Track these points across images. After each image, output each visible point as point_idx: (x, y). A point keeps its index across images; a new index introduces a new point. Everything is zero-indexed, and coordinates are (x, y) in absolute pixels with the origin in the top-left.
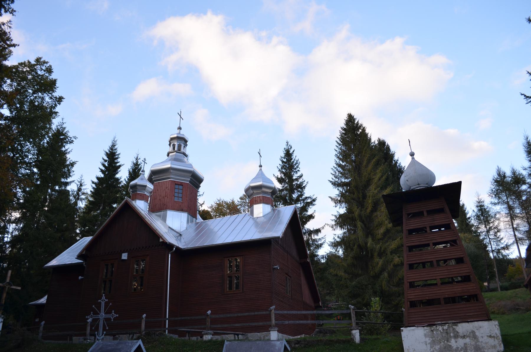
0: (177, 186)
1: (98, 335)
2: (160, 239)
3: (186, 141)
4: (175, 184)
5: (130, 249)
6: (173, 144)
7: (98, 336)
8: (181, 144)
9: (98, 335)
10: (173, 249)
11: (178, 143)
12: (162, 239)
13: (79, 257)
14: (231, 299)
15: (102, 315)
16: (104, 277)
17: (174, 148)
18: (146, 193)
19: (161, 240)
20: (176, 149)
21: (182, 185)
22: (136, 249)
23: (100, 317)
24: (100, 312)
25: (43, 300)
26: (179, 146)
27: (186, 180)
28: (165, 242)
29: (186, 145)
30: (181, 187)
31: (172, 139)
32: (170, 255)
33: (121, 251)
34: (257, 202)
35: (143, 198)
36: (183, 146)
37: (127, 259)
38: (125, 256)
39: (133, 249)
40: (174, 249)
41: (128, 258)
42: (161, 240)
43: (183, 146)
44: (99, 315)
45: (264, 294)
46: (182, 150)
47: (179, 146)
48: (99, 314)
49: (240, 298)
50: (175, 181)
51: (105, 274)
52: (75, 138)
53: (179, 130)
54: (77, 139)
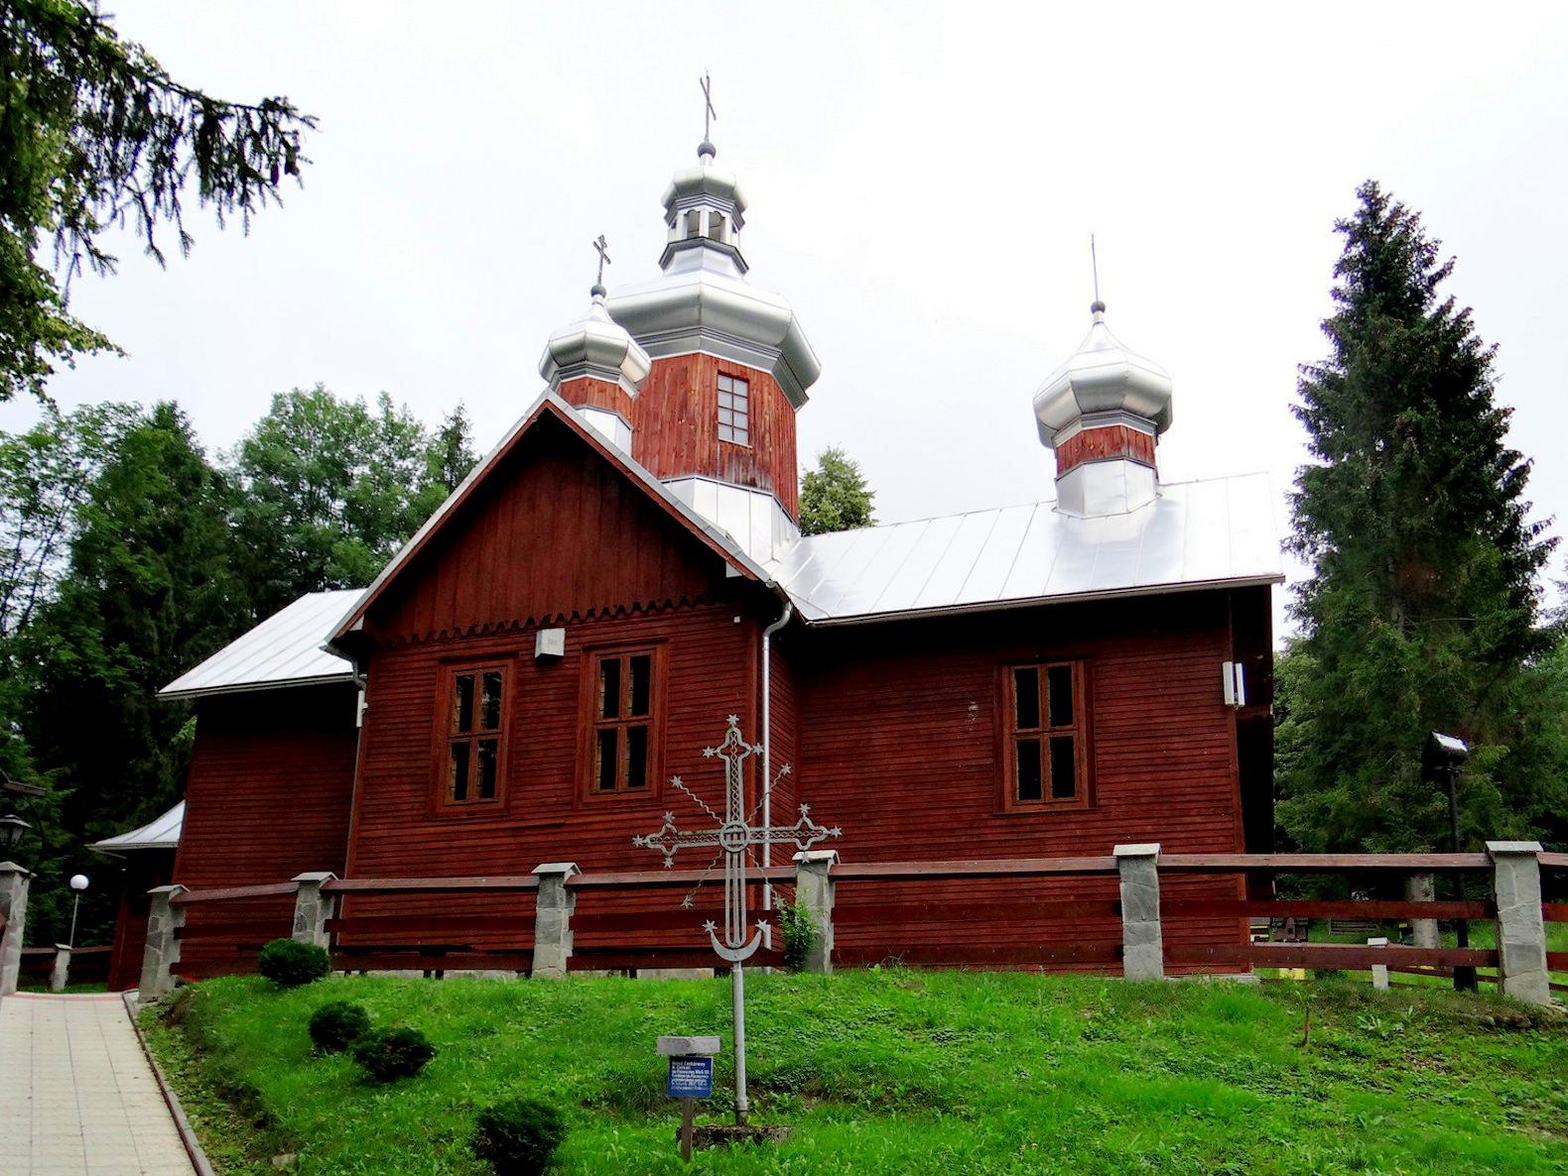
0: (724, 383)
1: (720, 936)
2: (729, 567)
3: (739, 208)
4: (720, 373)
5: (576, 615)
6: (686, 211)
7: (723, 943)
8: (723, 214)
9: (720, 936)
10: (780, 615)
11: (712, 210)
12: (738, 564)
13: (341, 644)
14: (1038, 835)
15: (736, 829)
16: (455, 729)
17: (693, 229)
18: (621, 383)
19: (731, 572)
20: (704, 231)
21: (747, 381)
22: (606, 611)
23: (725, 843)
24: (723, 814)
25: (167, 828)
26: (717, 223)
27: (764, 364)
28: (752, 578)
29: (739, 224)
30: (741, 388)
32: (766, 639)
33: (531, 621)
35: (611, 400)
36: (729, 223)
37: (562, 654)
38: (551, 642)
39: (591, 613)
40: (787, 614)
42: (731, 572)
43: (729, 223)
44: (722, 832)
45: (1198, 819)
46: (729, 238)
47: (717, 223)
48: (716, 825)
49: (1078, 832)
50: (717, 361)
51: (457, 717)
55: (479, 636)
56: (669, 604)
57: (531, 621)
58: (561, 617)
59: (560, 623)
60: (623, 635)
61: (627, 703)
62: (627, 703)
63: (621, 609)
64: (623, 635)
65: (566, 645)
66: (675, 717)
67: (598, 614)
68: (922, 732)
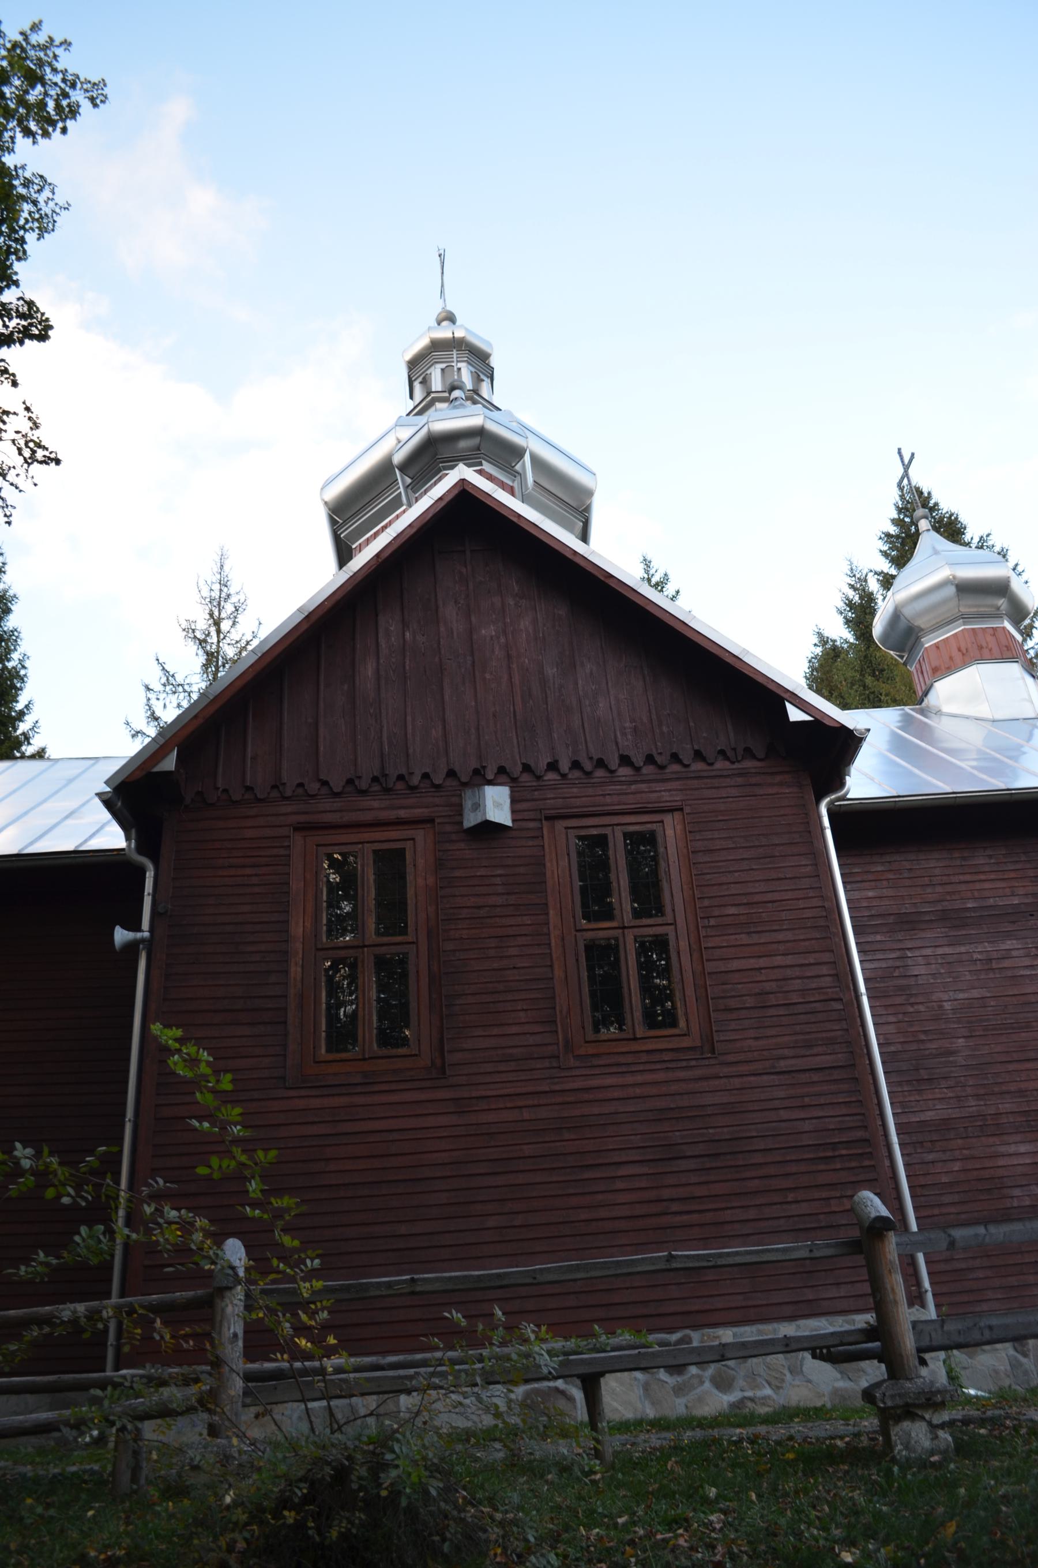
2: (788, 705)
6: (443, 366)
8: (482, 377)
22: (576, 765)
31: (437, 346)
33: (451, 774)
34: (986, 652)
37: (509, 823)
38: (498, 805)
39: (553, 766)
41: (514, 821)
52: (92, 100)
53: (445, 323)
54: (102, 106)
55: (363, 792)
56: (675, 758)
57: (451, 774)
58: (502, 770)
59: (503, 778)
60: (608, 800)
61: (623, 900)
62: (623, 900)
63: (601, 763)
64: (608, 800)
65: (513, 811)
66: (712, 922)
67: (565, 766)
68: (976, 956)
